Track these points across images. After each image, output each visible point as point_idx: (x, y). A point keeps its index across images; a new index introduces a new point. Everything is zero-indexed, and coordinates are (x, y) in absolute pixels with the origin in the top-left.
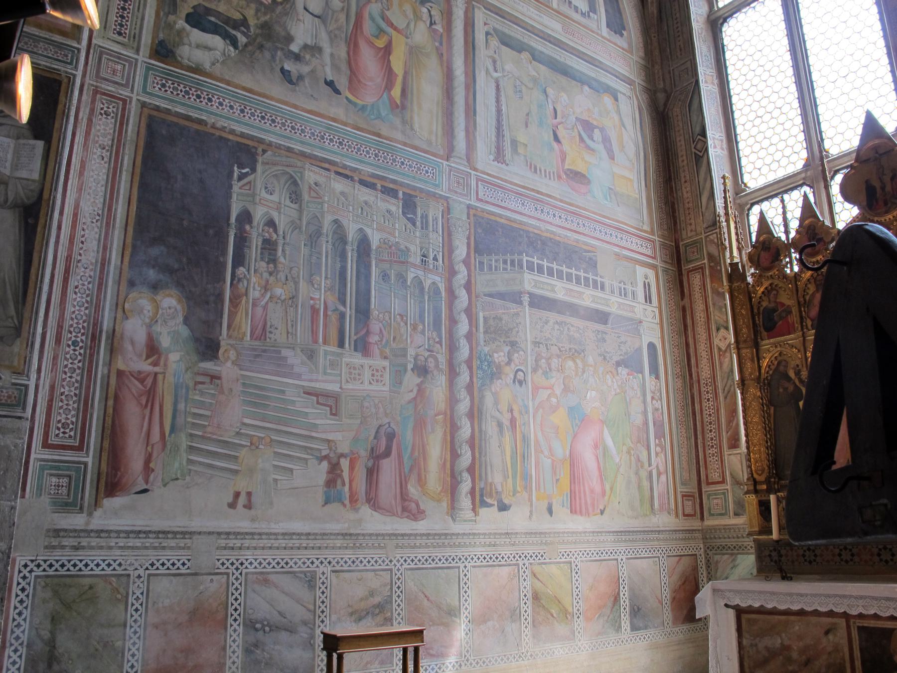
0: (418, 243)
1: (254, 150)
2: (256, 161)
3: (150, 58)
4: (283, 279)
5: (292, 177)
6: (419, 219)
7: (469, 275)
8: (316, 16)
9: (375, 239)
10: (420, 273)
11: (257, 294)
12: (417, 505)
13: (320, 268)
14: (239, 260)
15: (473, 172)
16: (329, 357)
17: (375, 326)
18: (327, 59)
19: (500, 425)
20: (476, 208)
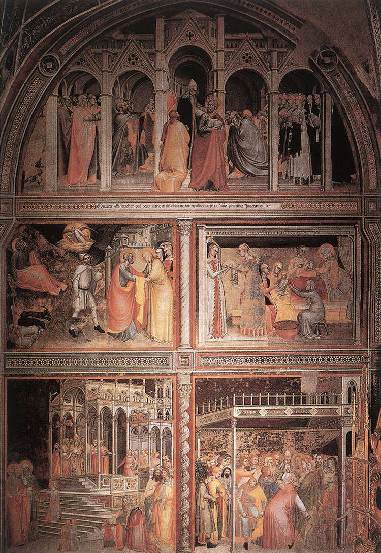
0: (156, 407)
1: (58, 382)
2: (60, 387)
3: (5, 351)
4: (77, 444)
5: (80, 390)
6: (156, 392)
7: (191, 418)
8: (86, 290)
9: (128, 411)
10: (157, 424)
11: (65, 454)
12: (156, 547)
13: (97, 436)
14: (55, 439)
15: (194, 351)
16: (104, 479)
17: (129, 459)
18: (94, 313)
19: (210, 502)
20: (197, 374)
